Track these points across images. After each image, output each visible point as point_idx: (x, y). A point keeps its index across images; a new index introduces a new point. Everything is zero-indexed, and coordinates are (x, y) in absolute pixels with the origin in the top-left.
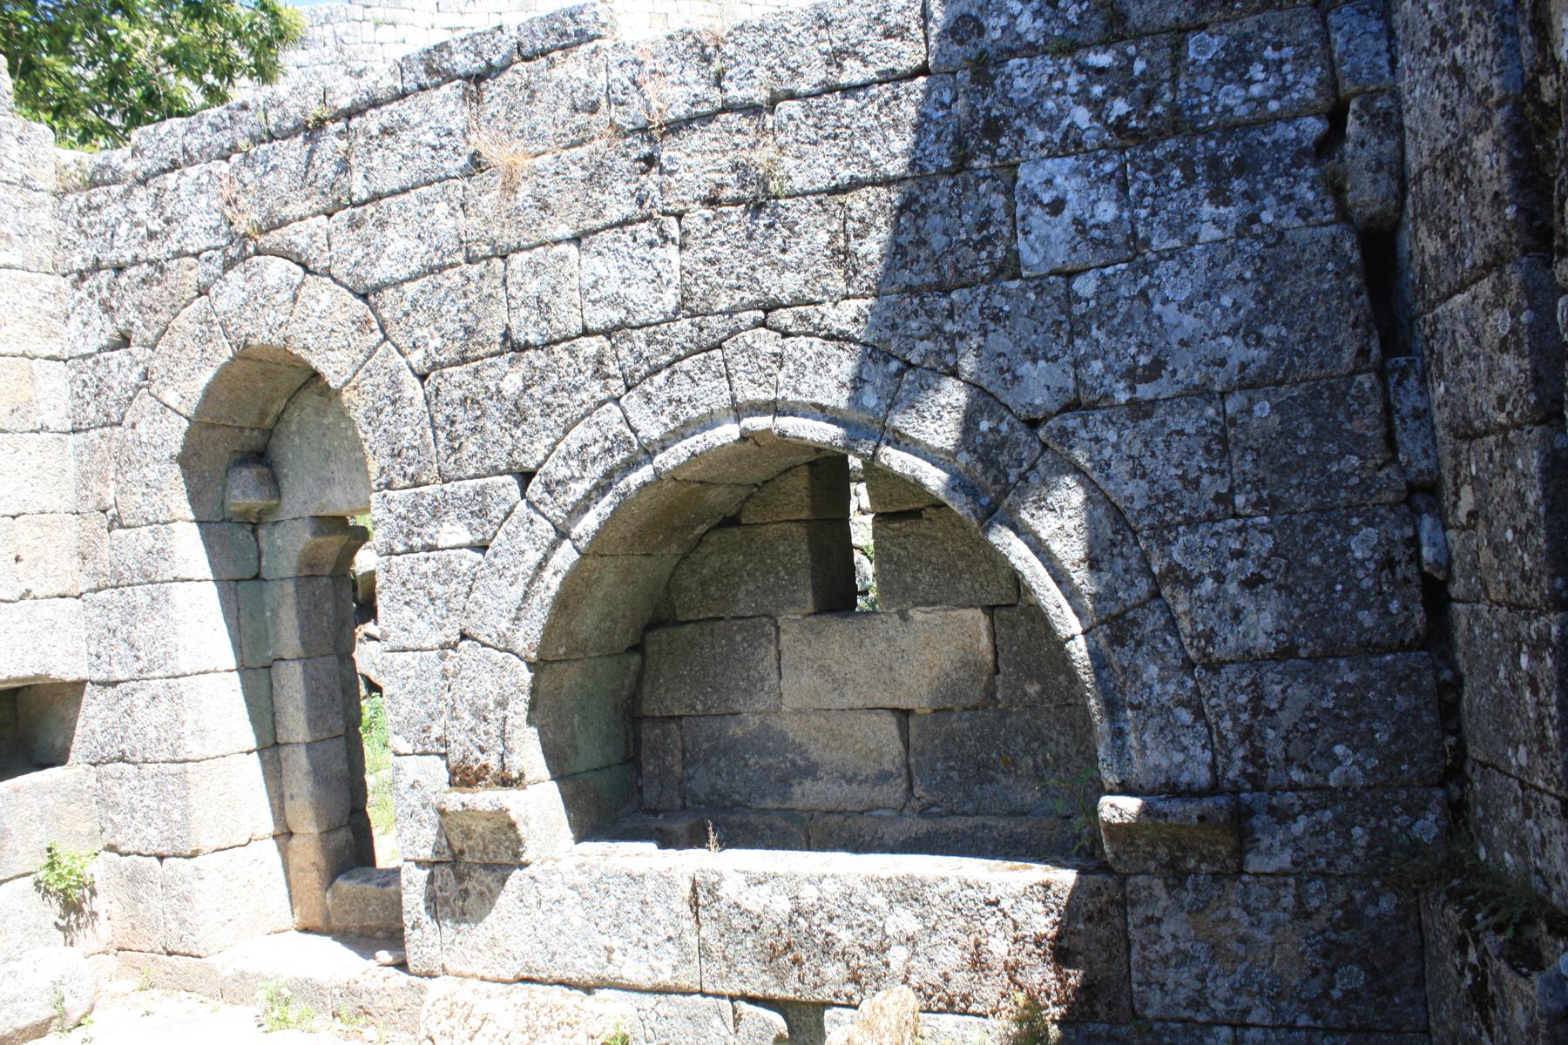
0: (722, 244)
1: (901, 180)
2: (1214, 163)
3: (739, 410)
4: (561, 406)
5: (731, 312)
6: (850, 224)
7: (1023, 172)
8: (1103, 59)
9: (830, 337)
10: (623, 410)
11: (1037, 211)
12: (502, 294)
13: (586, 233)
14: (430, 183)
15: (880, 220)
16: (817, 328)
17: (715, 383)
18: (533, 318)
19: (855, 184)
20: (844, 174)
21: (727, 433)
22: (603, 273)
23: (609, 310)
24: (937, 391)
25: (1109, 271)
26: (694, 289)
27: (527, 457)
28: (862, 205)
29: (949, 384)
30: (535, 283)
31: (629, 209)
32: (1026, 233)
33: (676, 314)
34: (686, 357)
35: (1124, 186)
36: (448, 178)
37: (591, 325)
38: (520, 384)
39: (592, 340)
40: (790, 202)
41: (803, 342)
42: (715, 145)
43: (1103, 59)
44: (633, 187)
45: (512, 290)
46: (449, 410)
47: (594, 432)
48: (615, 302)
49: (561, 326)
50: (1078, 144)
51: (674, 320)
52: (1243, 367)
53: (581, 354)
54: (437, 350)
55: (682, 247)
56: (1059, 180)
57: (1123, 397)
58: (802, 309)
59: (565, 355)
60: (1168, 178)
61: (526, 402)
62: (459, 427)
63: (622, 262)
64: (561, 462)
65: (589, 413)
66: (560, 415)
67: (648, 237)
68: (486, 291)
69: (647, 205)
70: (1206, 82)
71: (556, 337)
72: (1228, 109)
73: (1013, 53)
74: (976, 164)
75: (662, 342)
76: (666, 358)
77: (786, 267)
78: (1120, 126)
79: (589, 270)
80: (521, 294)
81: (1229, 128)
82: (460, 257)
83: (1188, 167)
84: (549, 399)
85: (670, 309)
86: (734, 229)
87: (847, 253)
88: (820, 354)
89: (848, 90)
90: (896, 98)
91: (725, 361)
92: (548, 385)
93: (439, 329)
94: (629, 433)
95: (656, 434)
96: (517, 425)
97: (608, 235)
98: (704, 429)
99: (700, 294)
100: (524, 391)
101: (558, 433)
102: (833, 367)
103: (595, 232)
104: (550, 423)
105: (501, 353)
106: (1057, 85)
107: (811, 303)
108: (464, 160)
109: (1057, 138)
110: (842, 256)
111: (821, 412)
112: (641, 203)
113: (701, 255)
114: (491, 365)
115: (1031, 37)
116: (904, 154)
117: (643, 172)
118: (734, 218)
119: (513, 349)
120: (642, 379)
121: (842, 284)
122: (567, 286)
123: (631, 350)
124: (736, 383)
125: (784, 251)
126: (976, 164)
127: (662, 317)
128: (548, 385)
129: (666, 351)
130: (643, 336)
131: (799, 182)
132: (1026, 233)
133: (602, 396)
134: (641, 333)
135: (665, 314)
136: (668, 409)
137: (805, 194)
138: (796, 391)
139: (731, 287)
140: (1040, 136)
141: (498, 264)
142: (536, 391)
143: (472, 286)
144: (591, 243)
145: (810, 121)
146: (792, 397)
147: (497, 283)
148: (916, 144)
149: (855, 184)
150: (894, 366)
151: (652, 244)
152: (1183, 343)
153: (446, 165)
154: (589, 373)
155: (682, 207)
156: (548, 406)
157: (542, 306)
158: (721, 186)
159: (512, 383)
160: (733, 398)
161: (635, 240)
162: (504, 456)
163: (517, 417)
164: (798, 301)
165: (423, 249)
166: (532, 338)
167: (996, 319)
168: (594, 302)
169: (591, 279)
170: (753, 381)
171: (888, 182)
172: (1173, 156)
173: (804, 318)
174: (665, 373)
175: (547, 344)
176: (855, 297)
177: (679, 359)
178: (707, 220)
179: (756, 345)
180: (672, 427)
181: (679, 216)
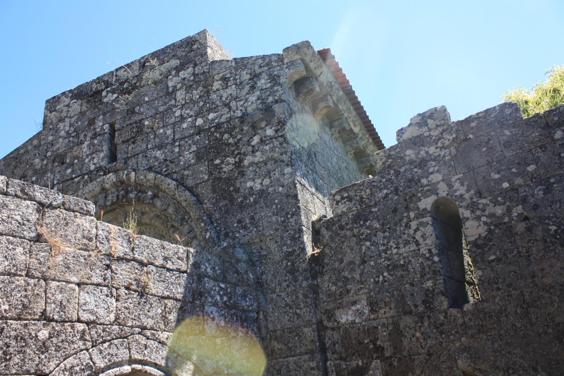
0: (131, 303)
1: (180, 300)
2: (241, 317)
3: (131, 361)
4: (65, 348)
5: (132, 327)
6: (167, 309)
7: (206, 307)
8: (223, 286)
9: (160, 342)
10: (90, 354)
11: (210, 319)
12: (43, 295)
13: (84, 283)
14: (15, 237)
15: (174, 310)
16: (157, 338)
17: (125, 350)
18: (57, 310)
19: (168, 298)
20: (166, 294)
21: (127, 369)
22: (89, 300)
23: (89, 315)
24: (186, 364)
25: (223, 338)
26: (121, 316)
27: (46, 368)
28: (170, 304)
29: (189, 363)
30: (60, 296)
31: (100, 280)
32: (207, 324)
33: (114, 323)
34: (116, 339)
35: (225, 318)
36: (25, 238)
37: (82, 319)
38: (47, 335)
39: (81, 325)
40: (151, 297)
41: (152, 342)
42: (129, 270)
43: (223, 286)
44: (103, 273)
45: (49, 295)
46: (7, 340)
47: (76, 361)
48: (92, 312)
49: (69, 316)
50: (217, 305)
51: (113, 325)
52: (247, 367)
53: (76, 329)
54: (5, 310)
55: (117, 300)
56: (214, 312)
57: (226, 372)
58: (153, 331)
59: (69, 328)
60: (233, 318)
61: (48, 343)
62: (11, 350)
63: (96, 299)
64: (61, 372)
65: (76, 353)
66: (64, 352)
67: (106, 293)
68: (36, 292)
69: (107, 281)
70: (240, 298)
71: (67, 320)
72: (243, 306)
73: (206, 277)
74: (196, 302)
75: (108, 332)
76: (109, 338)
77: (149, 317)
78: (225, 303)
79: (83, 298)
80: (53, 298)
81: (244, 311)
82: (24, 273)
83: (237, 317)
84: (60, 344)
85: (112, 320)
86: (135, 300)
87: (165, 317)
88: (157, 347)
89: (169, 270)
90: (180, 277)
91: (128, 343)
92: (60, 338)
93: (9, 302)
94: (92, 364)
95: (102, 366)
96: (43, 353)
97: (92, 287)
98: (117, 367)
99: (122, 318)
100: (49, 339)
101: (62, 359)
102: (161, 352)
103: (87, 284)
104: (59, 355)
105: (39, 320)
106: (214, 288)
107: (155, 330)
108: (33, 235)
109: (213, 301)
110: (164, 317)
111: (156, 366)
112: (105, 280)
113: (123, 305)
114: (34, 324)
115: (210, 274)
116: (181, 293)
117: (106, 270)
118: (135, 296)
119: (44, 320)
120: (99, 344)
121: (164, 327)
122: (74, 301)
123: (96, 332)
124: (132, 352)
125: (149, 312)
126: (196, 302)
127: (109, 323)
128: (60, 338)
129: (109, 335)
130: (101, 328)
131: (154, 291)
132: (207, 324)
133: (83, 347)
134: (101, 327)
135: (110, 322)
136: (108, 357)
137: (155, 296)
138: (150, 358)
139: (132, 319)
140: (210, 300)
141: (43, 283)
142: (54, 340)
143: (30, 288)
144: (85, 288)
145: (158, 274)
146: (149, 360)
147: (42, 290)
148: (184, 291)
149: (168, 298)
150: (176, 355)
151: (107, 296)
152: (236, 360)
153: (25, 233)
154: (78, 337)
155: (118, 286)
156: (59, 347)
157: (62, 306)
158: (131, 284)
159: (44, 334)
160: (130, 357)
161: (101, 292)
162: (34, 366)
163: (44, 350)
164: (152, 329)
165: (6, 263)
166: (56, 317)
167: (200, 346)
168: (84, 310)
169: (83, 301)
170: (137, 352)
171: (176, 300)
172: (234, 314)
173: (153, 334)
174: (107, 344)
175: (61, 322)
176: (167, 331)
177: (113, 339)
178: (126, 294)
179: (140, 340)
180: (108, 364)
181: (117, 289)
